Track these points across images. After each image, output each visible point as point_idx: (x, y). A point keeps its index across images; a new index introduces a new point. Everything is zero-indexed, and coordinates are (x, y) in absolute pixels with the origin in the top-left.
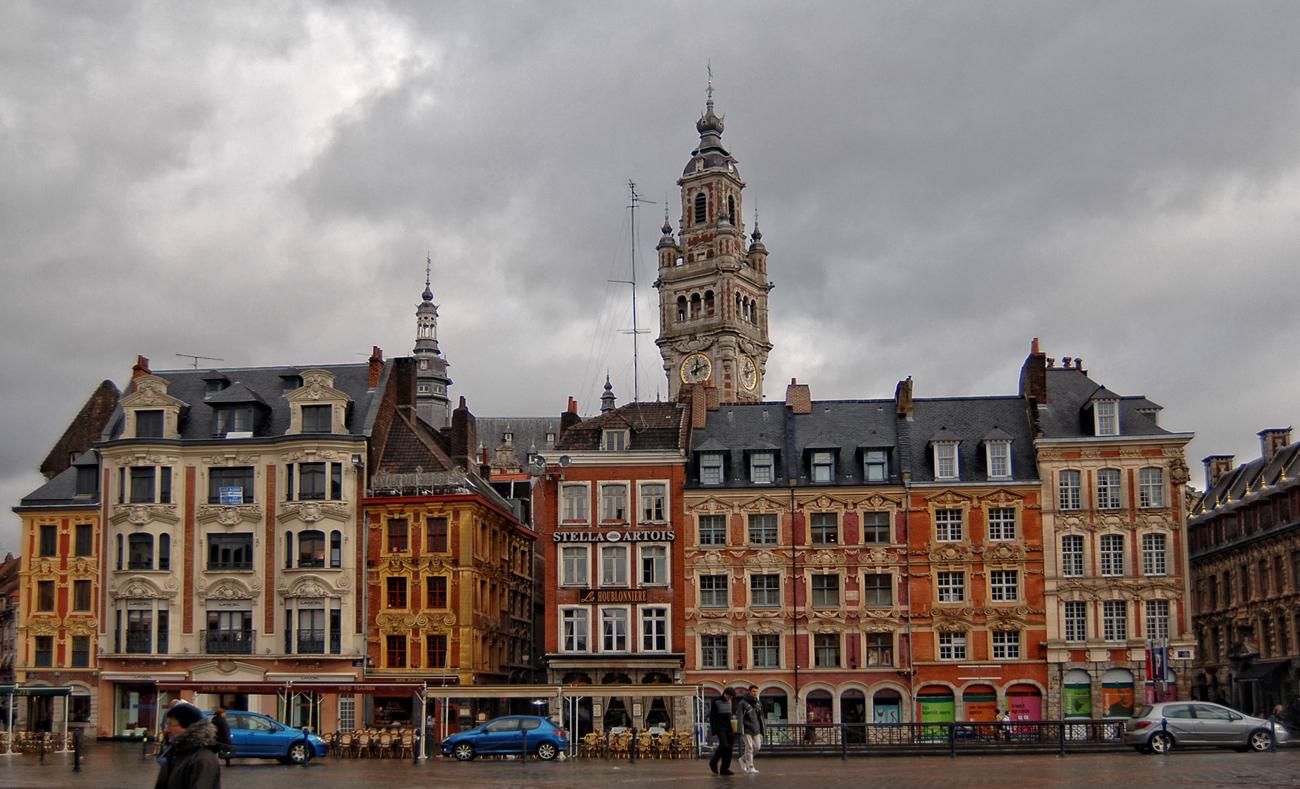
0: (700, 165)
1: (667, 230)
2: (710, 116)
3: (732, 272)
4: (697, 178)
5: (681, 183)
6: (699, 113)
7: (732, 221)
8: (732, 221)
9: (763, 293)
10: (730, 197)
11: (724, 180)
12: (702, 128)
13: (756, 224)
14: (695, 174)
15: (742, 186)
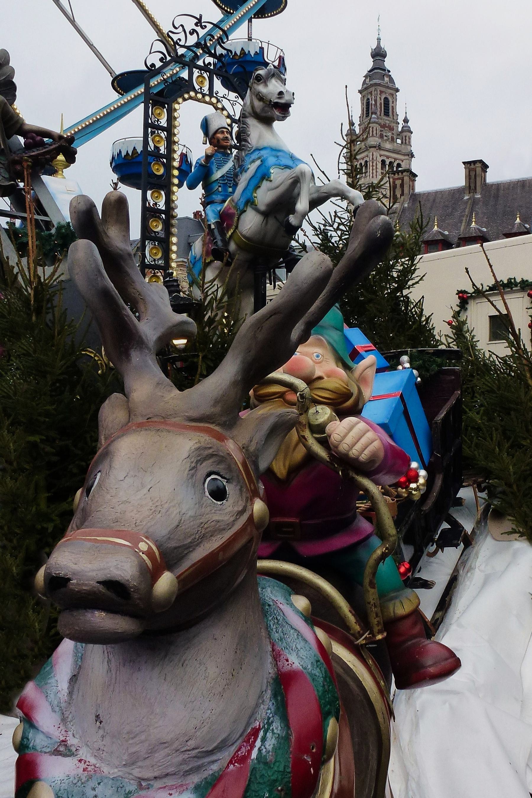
0: (368, 80)
1: (352, 124)
2: (379, 46)
3: (375, 147)
4: (366, 89)
5: (360, 92)
6: (374, 47)
7: (387, 114)
8: (387, 114)
9: (407, 157)
10: (386, 99)
11: (379, 88)
12: (373, 56)
13: (406, 113)
14: (365, 86)
15: (397, 90)
